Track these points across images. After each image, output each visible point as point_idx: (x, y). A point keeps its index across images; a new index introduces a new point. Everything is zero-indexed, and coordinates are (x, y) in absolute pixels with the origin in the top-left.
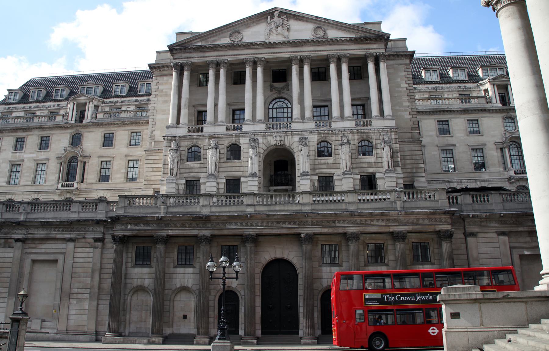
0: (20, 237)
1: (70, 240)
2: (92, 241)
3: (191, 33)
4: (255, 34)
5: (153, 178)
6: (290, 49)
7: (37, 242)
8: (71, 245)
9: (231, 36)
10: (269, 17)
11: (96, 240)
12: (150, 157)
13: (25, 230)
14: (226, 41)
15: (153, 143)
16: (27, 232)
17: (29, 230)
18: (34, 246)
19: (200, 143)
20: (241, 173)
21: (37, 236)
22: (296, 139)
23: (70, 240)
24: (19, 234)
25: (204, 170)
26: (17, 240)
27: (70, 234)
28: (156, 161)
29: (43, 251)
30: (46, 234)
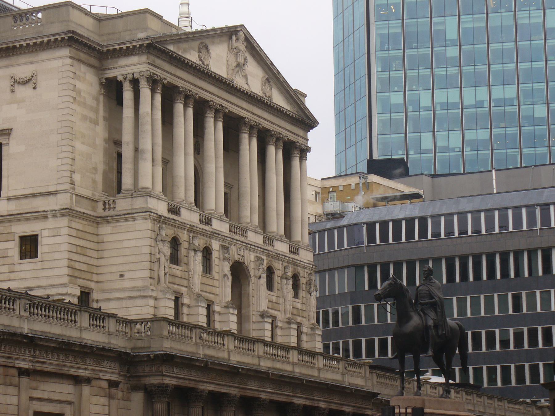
0: (25, 365)
1: (88, 381)
2: (105, 384)
3: (159, 17)
4: (219, 60)
5: (77, 265)
6: (244, 105)
7: (38, 378)
8: (86, 390)
9: (199, 52)
10: (234, 37)
11: (113, 384)
12: (74, 225)
13: (31, 353)
14: (193, 57)
15: (74, 196)
16: (34, 357)
17: (37, 353)
18: (34, 384)
19: (180, 234)
20: (213, 296)
21: (47, 368)
22: (252, 257)
23: (88, 381)
24: (25, 360)
25: (185, 282)
26: (23, 372)
27: (85, 369)
28: (80, 234)
29: (46, 395)
30: (59, 365)
